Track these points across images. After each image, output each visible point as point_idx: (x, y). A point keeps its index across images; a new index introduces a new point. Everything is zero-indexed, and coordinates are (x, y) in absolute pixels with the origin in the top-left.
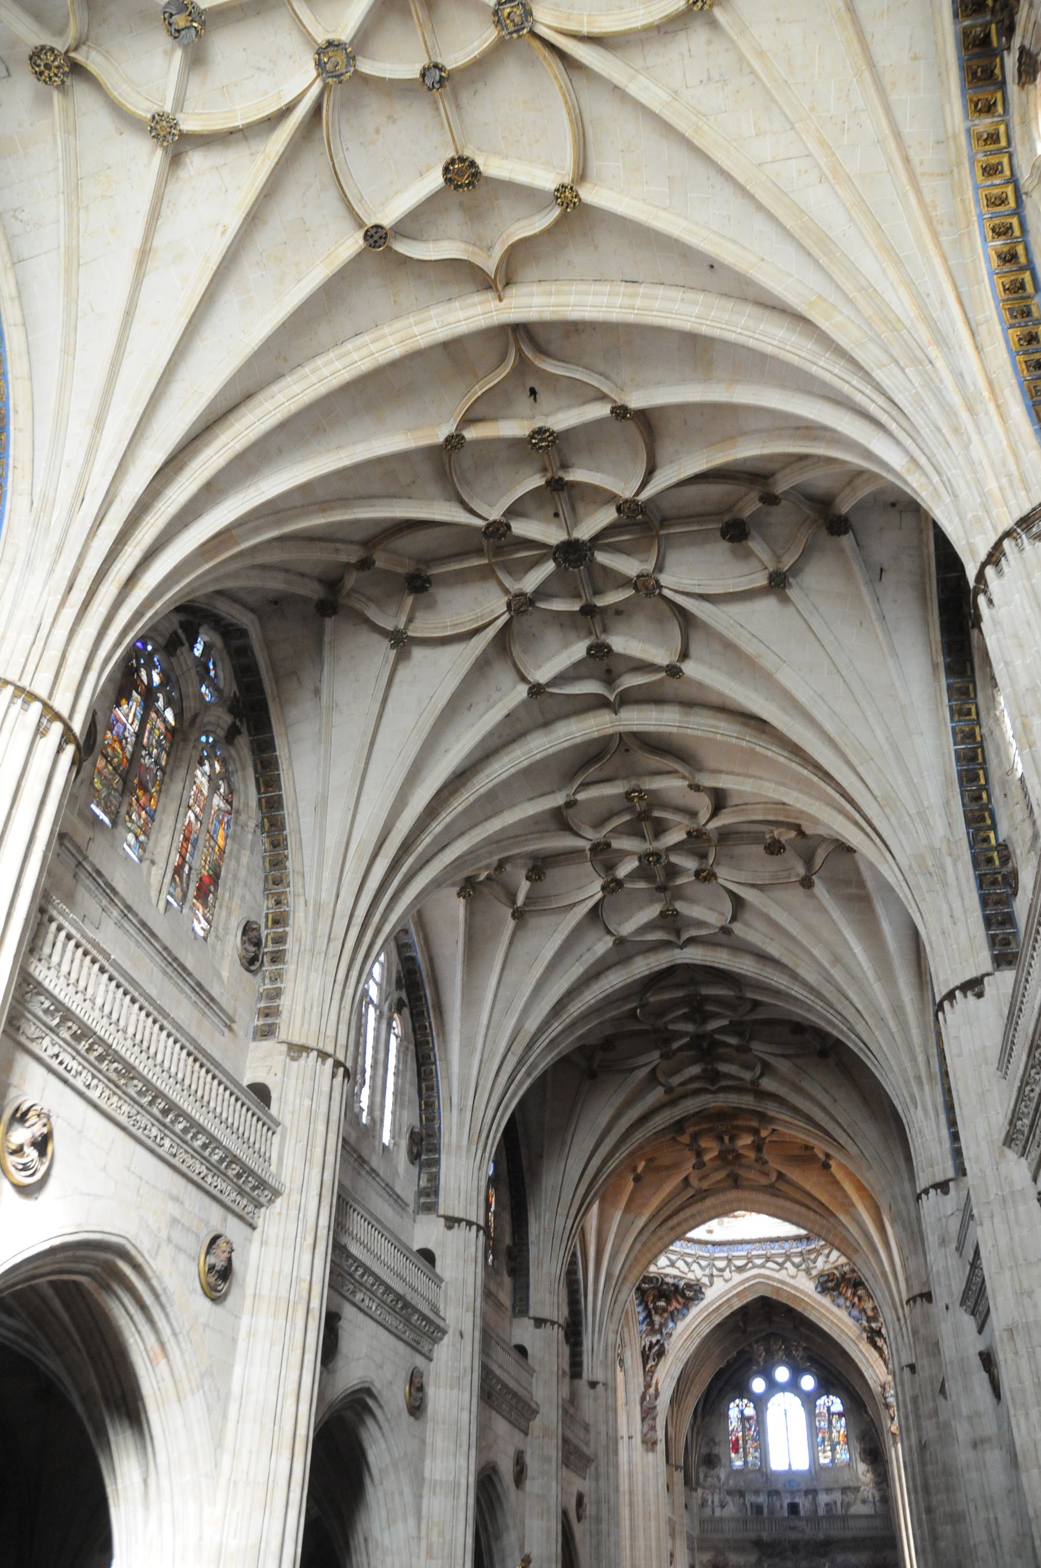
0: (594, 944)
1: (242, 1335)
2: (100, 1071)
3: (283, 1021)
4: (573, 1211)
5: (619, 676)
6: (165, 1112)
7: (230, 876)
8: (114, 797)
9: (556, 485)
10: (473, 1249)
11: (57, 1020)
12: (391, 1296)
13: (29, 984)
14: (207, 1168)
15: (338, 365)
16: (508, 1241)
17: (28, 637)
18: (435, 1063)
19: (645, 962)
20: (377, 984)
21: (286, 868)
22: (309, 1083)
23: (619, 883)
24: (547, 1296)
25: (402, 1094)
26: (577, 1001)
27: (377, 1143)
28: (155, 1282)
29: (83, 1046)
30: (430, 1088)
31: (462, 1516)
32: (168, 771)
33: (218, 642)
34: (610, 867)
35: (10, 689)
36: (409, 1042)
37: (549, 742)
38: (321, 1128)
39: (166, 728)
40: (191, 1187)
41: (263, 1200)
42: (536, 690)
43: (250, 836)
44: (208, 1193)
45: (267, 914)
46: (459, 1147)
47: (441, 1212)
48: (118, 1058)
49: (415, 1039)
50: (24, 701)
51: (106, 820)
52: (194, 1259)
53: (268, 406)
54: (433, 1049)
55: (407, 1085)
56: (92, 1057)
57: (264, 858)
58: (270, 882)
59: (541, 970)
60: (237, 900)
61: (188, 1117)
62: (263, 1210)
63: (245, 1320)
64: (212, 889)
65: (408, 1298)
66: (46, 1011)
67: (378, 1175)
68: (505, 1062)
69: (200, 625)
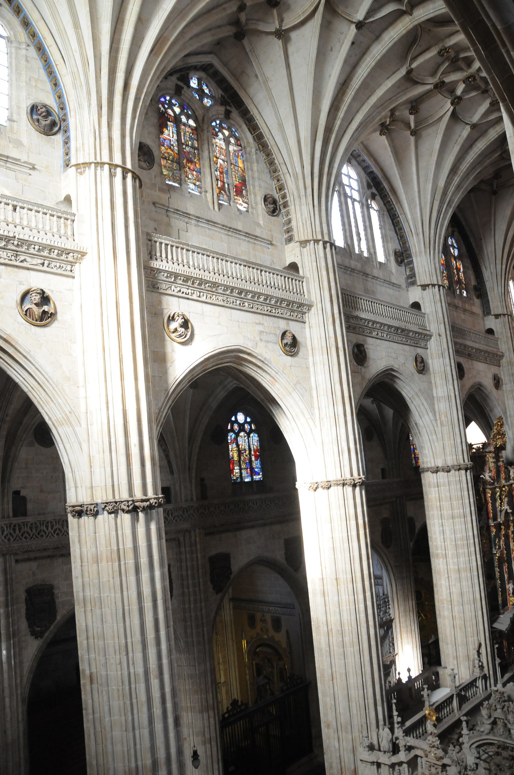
0: (462, 132)
1: (311, 364)
2: (202, 289)
3: (295, 233)
6: (240, 293)
7: (250, 179)
10: (438, 296)
11: (173, 278)
13: (154, 271)
16: (473, 282)
17: (92, 139)
18: (399, 217)
19: (494, 131)
20: (357, 191)
22: (313, 256)
23: (460, 98)
24: (499, 303)
26: (463, 163)
27: (375, 264)
28: (259, 357)
29: (190, 283)
30: (401, 229)
31: (454, 408)
32: (200, 148)
33: (203, 74)
34: (452, 91)
35: (93, 165)
36: (383, 211)
37: (382, 47)
38: (324, 273)
39: (192, 130)
40: (265, 317)
41: (304, 310)
42: (360, 25)
43: (254, 156)
44: (275, 316)
45: (276, 187)
46: (420, 252)
47: (419, 284)
48: (207, 282)
49: (387, 208)
50: (101, 167)
51: (176, 185)
52: (276, 343)
54: (396, 210)
55: (388, 231)
56: (196, 285)
57: (265, 162)
58: (272, 172)
59: (436, 156)
60: (257, 188)
61: (251, 292)
62: (307, 314)
63: (311, 359)
64: (243, 188)
65: (403, 327)
66: (167, 277)
67: (378, 278)
68: (434, 205)
69: (188, 74)
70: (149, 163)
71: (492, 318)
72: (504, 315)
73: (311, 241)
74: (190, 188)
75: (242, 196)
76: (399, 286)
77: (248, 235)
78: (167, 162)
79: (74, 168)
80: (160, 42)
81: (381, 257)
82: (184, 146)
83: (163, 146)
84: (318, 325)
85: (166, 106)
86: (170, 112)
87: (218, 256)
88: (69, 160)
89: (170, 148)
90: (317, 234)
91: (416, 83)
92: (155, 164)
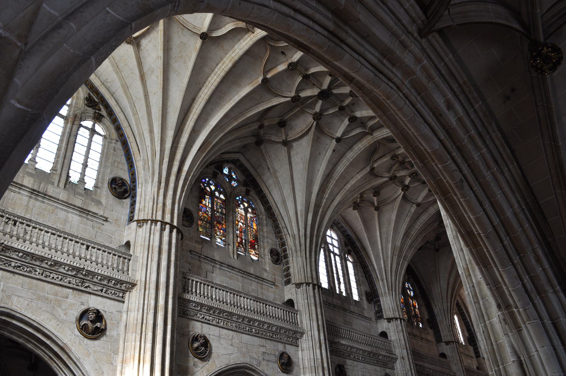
3: (292, 277)
4: (449, 300)
5: (366, 123)
6: (249, 321)
8: (209, 231)
9: (306, 77)
10: (400, 327)
11: (199, 308)
12: (366, 353)
13: (185, 301)
14: (272, 333)
15: (215, 77)
17: (151, 204)
20: (337, 248)
21: (280, 227)
22: (305, 295)
24: (448, 333)
25: (359, 281)
29: (211, 312)
32: (226, 214)
33: (232, 166)
34: (402, 182)
35: (150, 222)
37: (353, 153)
38: (313, 308)
39: (222, 201)
41: (298, 337)
42: (338, 140)
44: (275, 341)
45: (279, 244)
47: (385, 317)
48: (224, 311)
49: (359, 261)
50: (155, 223)
52: (275, 362)
53: (200, 100)
55: (360, 278)
57: (272, 226)
60: (266, 244)
62: (300, 340)
65: (374, 351)
66: (195, 306)
67: (354, 312)
69: (222, 165)
70: (189, 223)
71: (443, 344)
72: (453, 342)
73: (304, 283)
74: (217, 242)
75: (254, 249)
76: (370, 319)
77: (257, 277)
78: (203, 223)
79: (135, 222)
80: (206, 144)
81: (356, 297)
82: (216, 212)
83: (201, 211)
84: (308, 349)
85: (206, 185)
86: (208, 189)
87: (234, 292)
88: (133, 217)
89: (206, 213)
90: (309, 278)
91: (377, 176)
92: (194, 224)
